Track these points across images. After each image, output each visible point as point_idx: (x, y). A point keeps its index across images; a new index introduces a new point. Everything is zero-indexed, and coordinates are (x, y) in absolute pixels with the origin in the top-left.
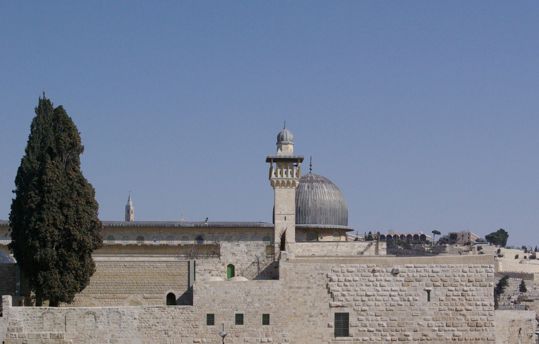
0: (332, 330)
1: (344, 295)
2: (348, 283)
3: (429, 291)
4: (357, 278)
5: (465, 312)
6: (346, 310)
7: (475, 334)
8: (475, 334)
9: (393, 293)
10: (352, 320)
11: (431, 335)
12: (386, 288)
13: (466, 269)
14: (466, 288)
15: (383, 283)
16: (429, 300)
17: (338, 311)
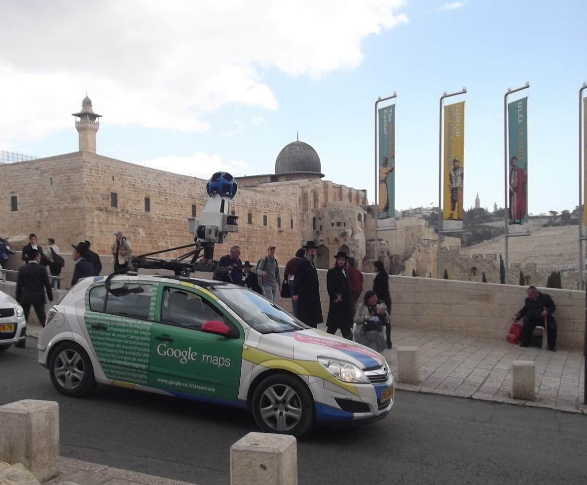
0: (10, 208)
1: (14, 185)
2: (15, 177)
3: (51, 178)
4: (19, 174)
5: (68, 191)
6: (16, 195)
7: (75, 205)
8: (75, 205)
9: (35, 181)
10: (19, 200)
11: (54, 207)
12: (32, 179)
13: (69, 162)
14: (69, 175)
15: (31, 176)
16: (52, 184)
17: (12, 195)
